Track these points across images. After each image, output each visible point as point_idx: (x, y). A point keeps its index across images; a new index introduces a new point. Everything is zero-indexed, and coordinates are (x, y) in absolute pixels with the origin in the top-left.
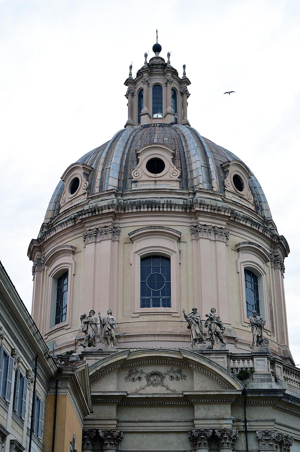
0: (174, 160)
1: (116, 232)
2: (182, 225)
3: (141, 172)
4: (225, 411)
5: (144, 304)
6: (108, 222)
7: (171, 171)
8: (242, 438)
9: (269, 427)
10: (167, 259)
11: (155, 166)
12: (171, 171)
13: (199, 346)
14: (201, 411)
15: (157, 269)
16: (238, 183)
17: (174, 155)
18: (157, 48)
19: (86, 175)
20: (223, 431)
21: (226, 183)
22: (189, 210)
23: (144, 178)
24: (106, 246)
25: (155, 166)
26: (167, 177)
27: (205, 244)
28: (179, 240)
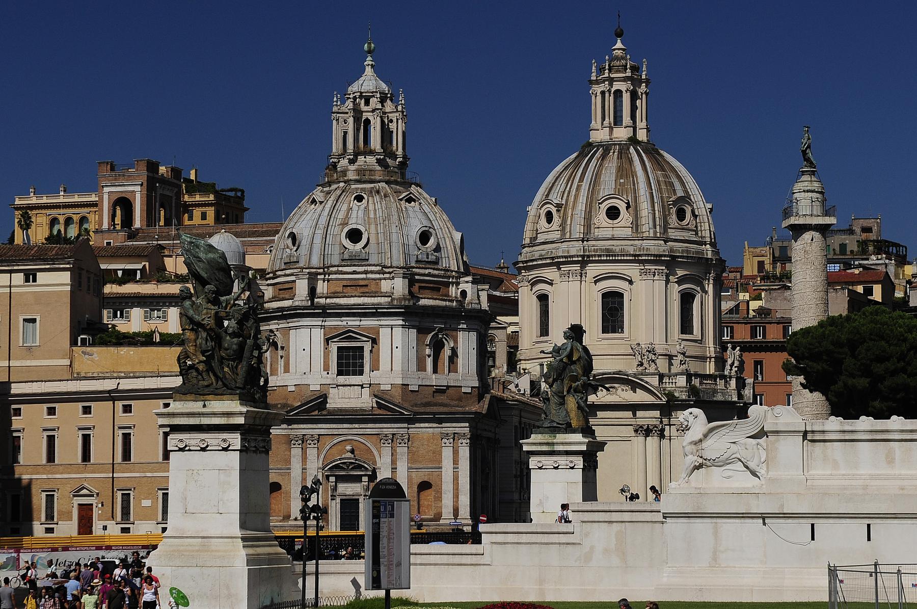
2: (632, 270)
3: (601, 218)
6: (577, 267)
8: (667, 428)
10: (621, 295)
11: (613, 213)
13: (640, 369)
14: (639, 414)
15: (613, 303)
16: (681, 215)
17: (628, 203)
20: (655, 426)
21: (670, 221)
22: (636, 259)
23: (604, 224)
25: (613, 213)
26: (622, 224)
28: (631, 282)
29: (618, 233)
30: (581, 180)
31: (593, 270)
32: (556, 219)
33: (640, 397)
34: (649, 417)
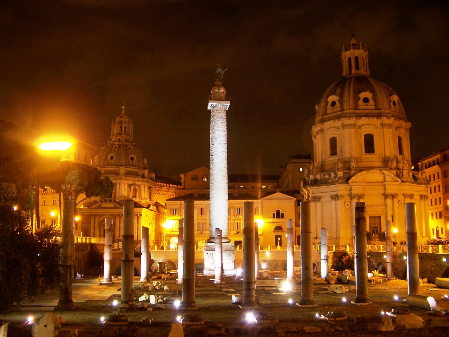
12: (372, 102)
19: (339, 101)
29: (369, 107)
30: (349, 87)
32: (338, 104)
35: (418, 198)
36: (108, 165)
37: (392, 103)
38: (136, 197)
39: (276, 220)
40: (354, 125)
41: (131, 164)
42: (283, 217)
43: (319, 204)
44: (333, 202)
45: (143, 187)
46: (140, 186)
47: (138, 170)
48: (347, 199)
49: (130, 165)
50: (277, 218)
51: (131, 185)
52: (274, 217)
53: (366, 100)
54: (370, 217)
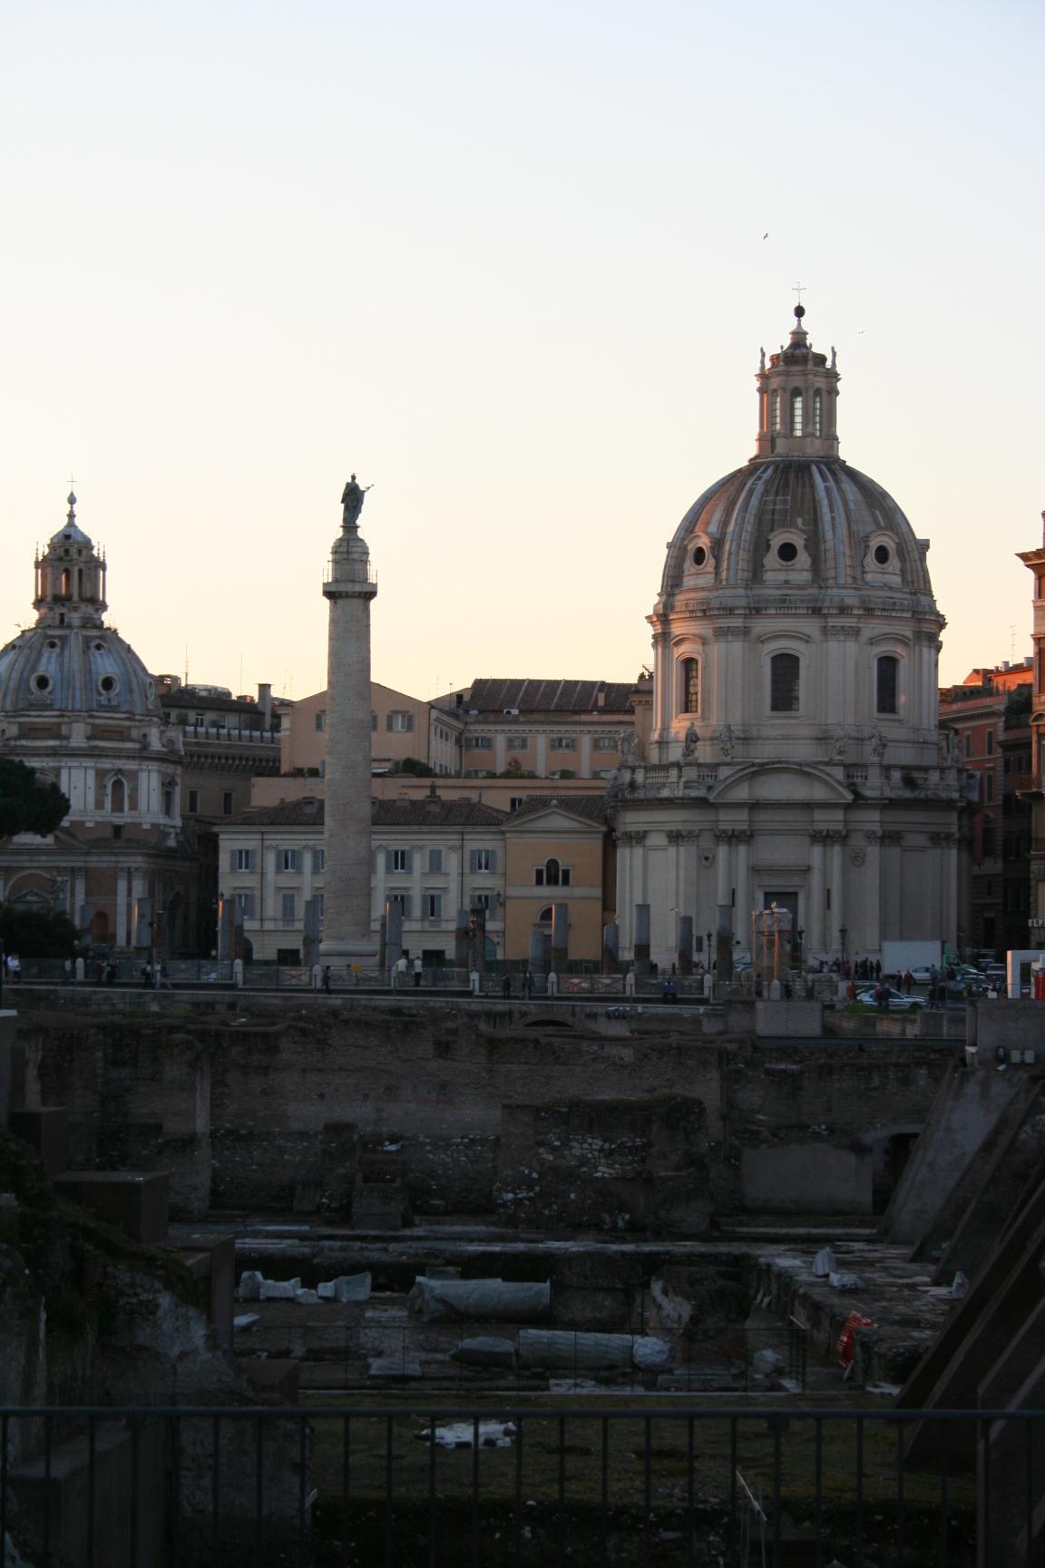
0: (806, 546)
1: (745, 632)
2: (811, 627)
3: (772, 559)
4: (839, 815)
5: (775, 708)
6: (737, 622)
7: (803, 559)
9: (876, 827)
10: (796, 659)
11: (788, 552)
12: (803, 559)
14: (819, 815)
18: (800, 312)
24: (737, 647)
26: (798, 566)
27: (834, 646)
31: (761, 626)
32: (709, 561)
33: (819, 793)
34: (831, 820)
35: (922, 840)
36: (31, 707)
37: (871, 558)
38: (121, 809)
39: (545, 891)
40: (745, 632)
41: (105, 702)
42: (566, 882)
43: (638, 851)
44: (672, 850)
45: (143, 777)
46: (133, 775)
47: (128, 723)
48: (706, 842)
49: (101, 707)
50: (549, 883)
51: (106, 772)
52: (539, 882)
53: (788, 552)
54: (766, 894)
